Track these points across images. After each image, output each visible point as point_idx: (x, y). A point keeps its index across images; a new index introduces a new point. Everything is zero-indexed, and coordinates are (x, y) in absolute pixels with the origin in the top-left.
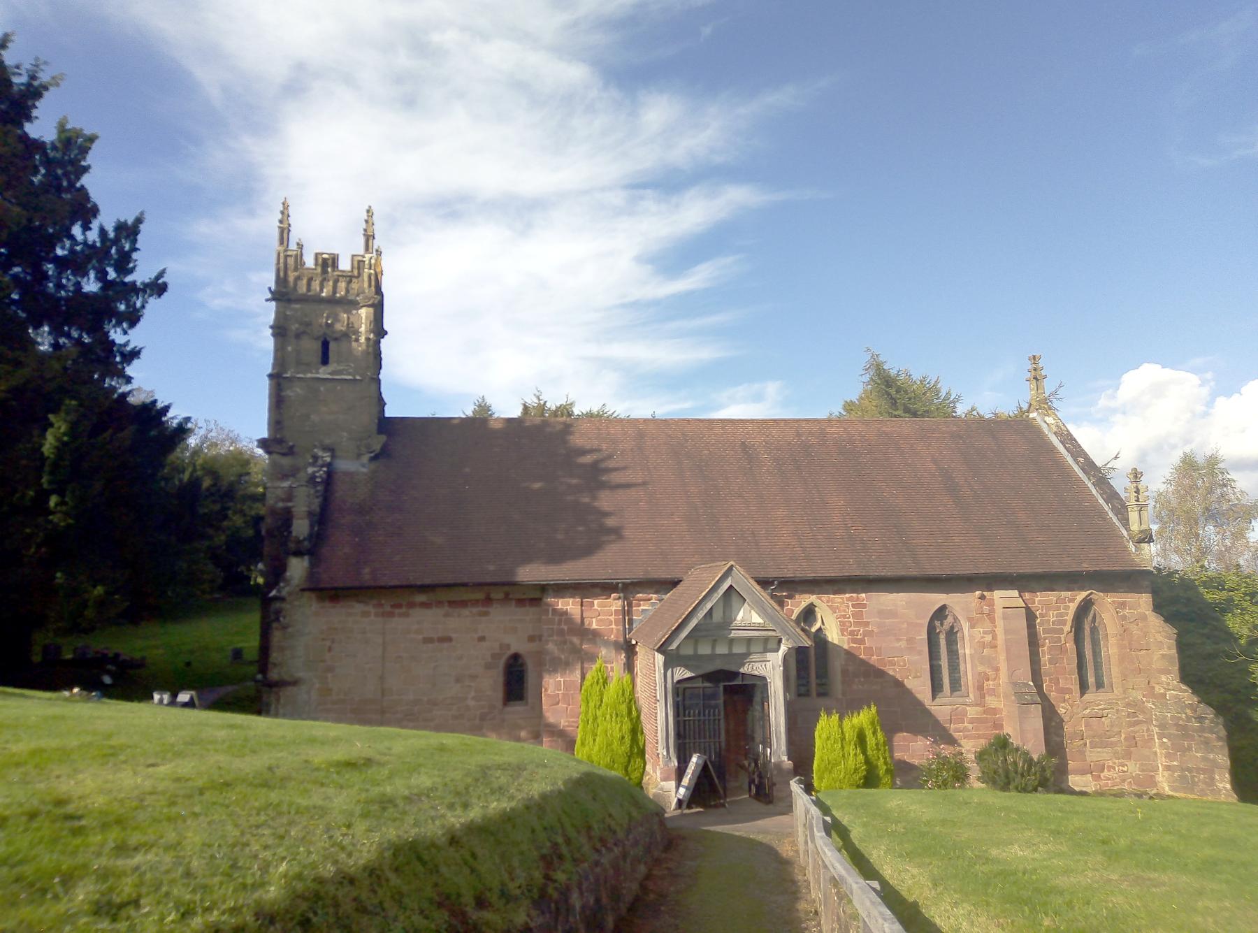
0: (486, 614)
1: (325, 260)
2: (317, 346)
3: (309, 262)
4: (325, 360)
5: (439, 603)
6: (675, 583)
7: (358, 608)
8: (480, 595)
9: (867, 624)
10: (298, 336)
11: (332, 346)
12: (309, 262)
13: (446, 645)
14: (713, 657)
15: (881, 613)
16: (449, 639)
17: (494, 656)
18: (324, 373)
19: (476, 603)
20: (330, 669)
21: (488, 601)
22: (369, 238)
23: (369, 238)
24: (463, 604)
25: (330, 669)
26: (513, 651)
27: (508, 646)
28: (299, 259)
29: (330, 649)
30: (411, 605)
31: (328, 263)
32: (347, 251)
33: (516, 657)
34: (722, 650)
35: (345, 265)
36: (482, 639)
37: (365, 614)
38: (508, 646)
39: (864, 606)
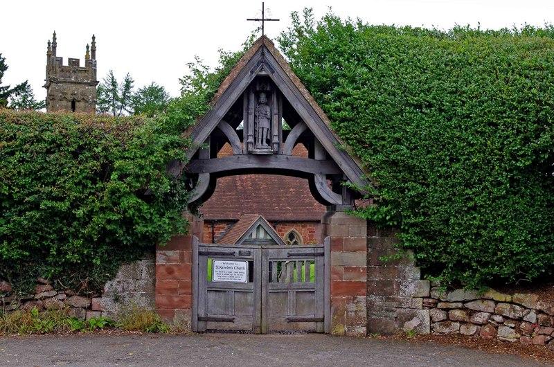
2: (70, 104)
3: (65, 63)
6: (235, 221)
11: (77, 104)
12: (65, 63)
31: (74, 62)
35: (82, 64)
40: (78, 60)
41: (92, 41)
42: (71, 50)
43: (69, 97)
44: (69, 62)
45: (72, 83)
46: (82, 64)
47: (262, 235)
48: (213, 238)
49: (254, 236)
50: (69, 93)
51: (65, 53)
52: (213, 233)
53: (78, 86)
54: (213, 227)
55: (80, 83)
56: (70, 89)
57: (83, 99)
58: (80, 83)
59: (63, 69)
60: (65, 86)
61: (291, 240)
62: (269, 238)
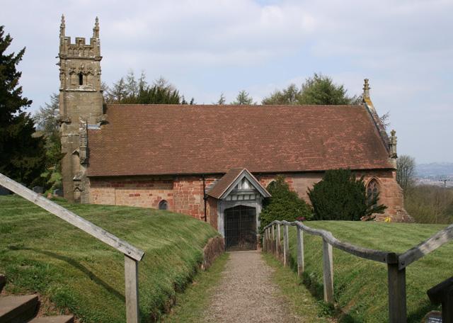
0: (153, 186)
1: (80, 41)
2: (78, 77)
3: (73, 42)
4: (81, 83)
5: (135, 182)
7: (106, 183)
8: (150, 179)
10: (71, 74)
11: (84, 76)
12: (73, 42)
13: (138, 197)
15: (298, 184)
16: (139, 195)
17: (156, 201)
18: (81, 88)
19: (148, 182)
21: (153, 181)
24: (144, 182)
26: (163, 199)
27: (161, 198)
28: (69, 39)
29: (96, 199)
30: (125, 183)
31: (80, 41)
32: (88, 36)
33: (164, 201)
35: (88, 43)
36: (151, 195)
37: (108, 186)
38: (161, 198)
40: (84, 39)
41: (95, 22)
42: (79, 30)
43: (77, 71)
44: (76, 41)
45: (80, 58)
46: (88, 43)
47: (246, 186)
48: (204, 189)
49: (240, 188)
50: (77, 68)
51: (72, 34)
52: (204, 185)
53: (85, 61)
54: (204, 180)
55: (86, 59)
56: (78, 64)
57: (89, 72)
58: (86, 59)
59: (71, 47)
60: (74, 61)
62: (253, 188)
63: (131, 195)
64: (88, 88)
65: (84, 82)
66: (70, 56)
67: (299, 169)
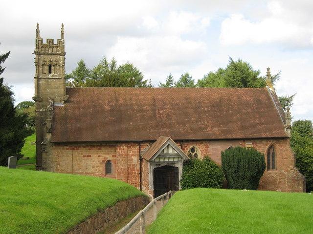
3: (45, 42)
4: (50, 72)
5: (87, 146)
9: (209, 152)
12: (45, 42)
14: (164, 162)
18: (50, 76)
19: (97, 146)
20: (59, 164)
21: (101, 146)
22: (62, 33)
23: (62, 33)
24: (94, 146)
25: (59, 164)
29: (58, 158)
31: (50, 41)
32: (56, 37)
33: (109, 161)
34: (166, 160)
35: (55, 42)
36: (99, 156)
37: (67, 149)
39: (208, 147)
45: (49, 54)
52: (140, 149)
54: (140, 145)
58: (54, 54)
59: (43, 46)
61: (193, 153)
63: (84, 156)
64: (55, 76)
65: (52, 71)
66: (42, 52)
67: (213, 137)
